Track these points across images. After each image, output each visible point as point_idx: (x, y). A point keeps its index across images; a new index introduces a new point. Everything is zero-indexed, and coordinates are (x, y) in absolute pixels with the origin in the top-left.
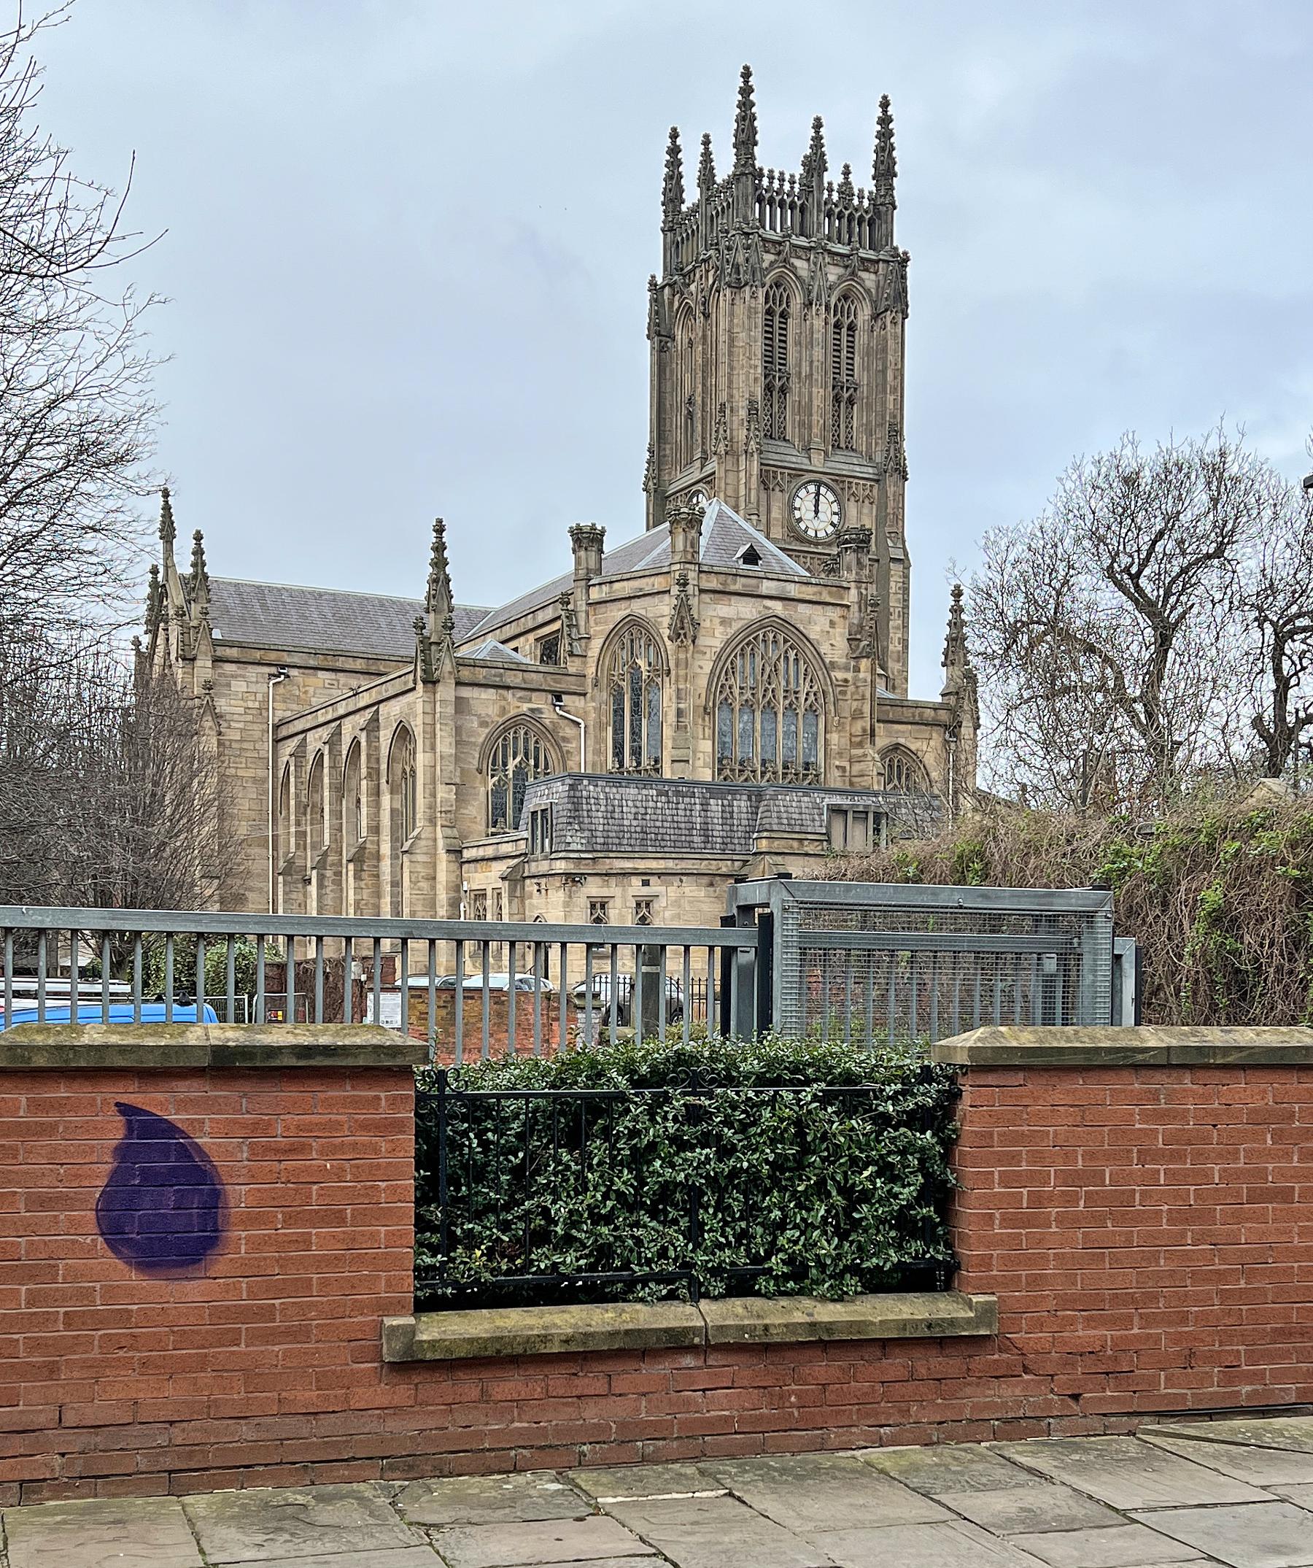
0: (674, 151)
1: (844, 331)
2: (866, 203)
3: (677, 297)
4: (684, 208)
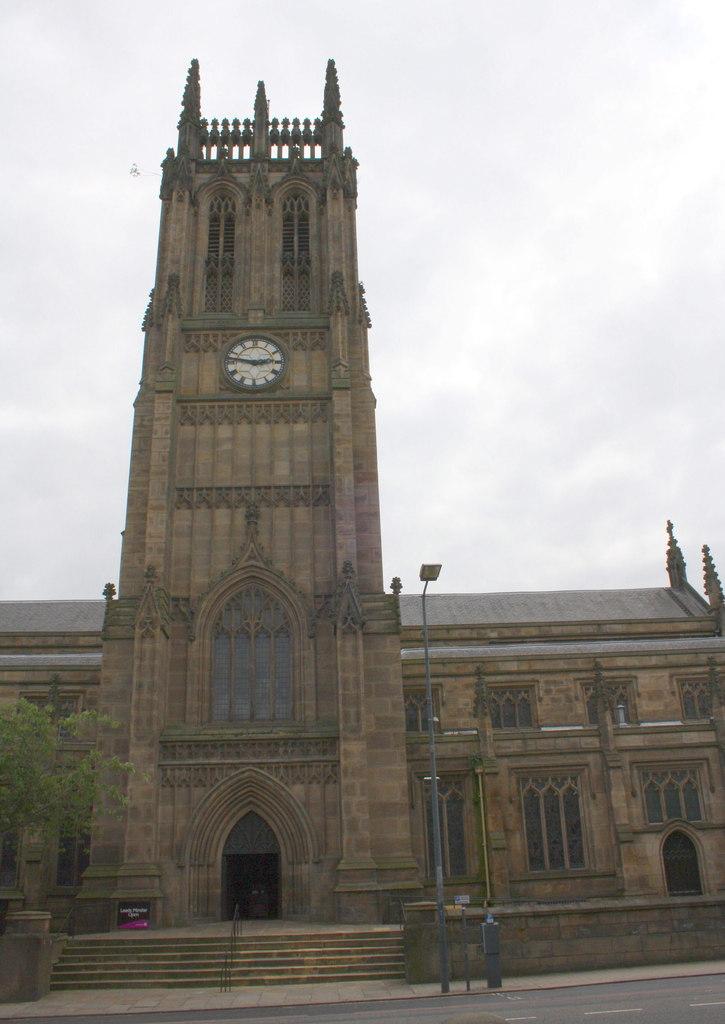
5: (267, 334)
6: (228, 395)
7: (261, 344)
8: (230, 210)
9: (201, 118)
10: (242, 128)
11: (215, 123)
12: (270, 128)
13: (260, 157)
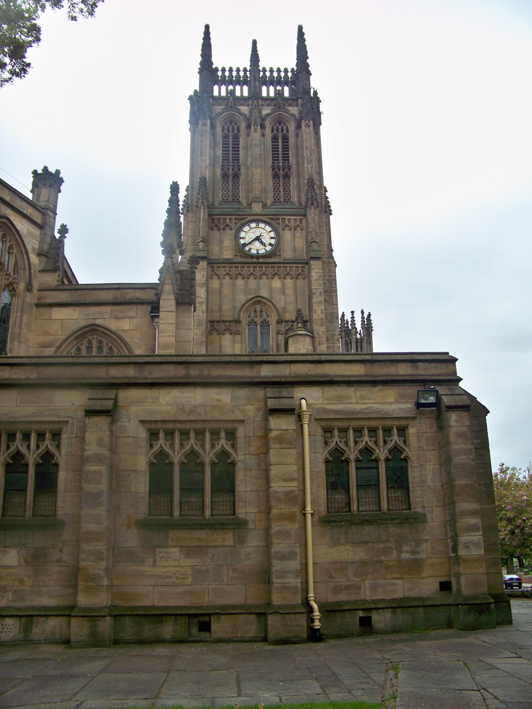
1: (280, 140)
7: (262, 225)
8: (235, 131)
9: (214, 67)
10: (242, 74)
12: (261, 74)
13: (255, 95)
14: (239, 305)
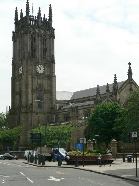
0: (16, 11)
2: (48, 21)
3: (17, 34)
4: (18, 20)
5: (41, 64)
6: (37, 75)
9: (30, 15)
11: (32, 16)
14: (36, 86)
